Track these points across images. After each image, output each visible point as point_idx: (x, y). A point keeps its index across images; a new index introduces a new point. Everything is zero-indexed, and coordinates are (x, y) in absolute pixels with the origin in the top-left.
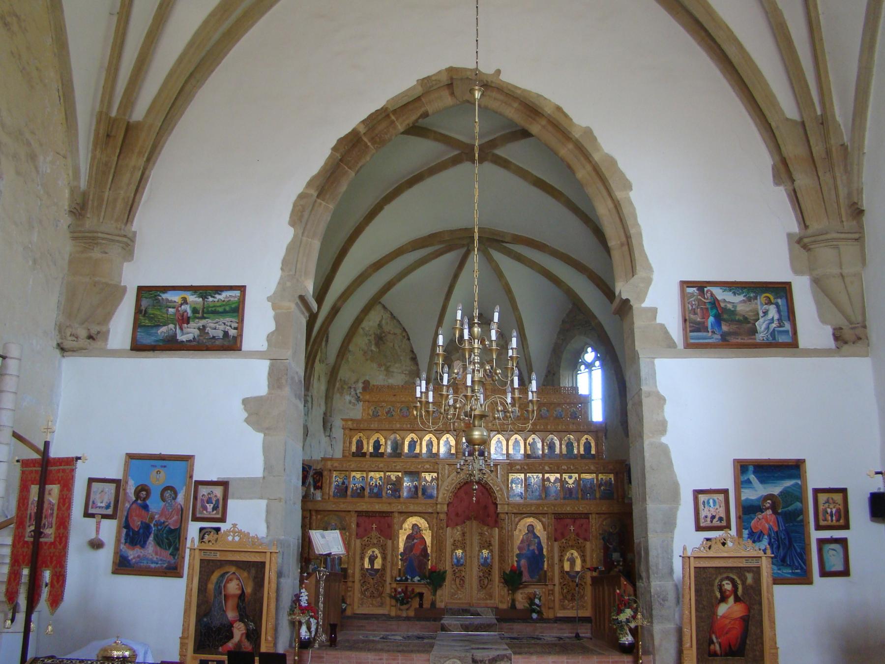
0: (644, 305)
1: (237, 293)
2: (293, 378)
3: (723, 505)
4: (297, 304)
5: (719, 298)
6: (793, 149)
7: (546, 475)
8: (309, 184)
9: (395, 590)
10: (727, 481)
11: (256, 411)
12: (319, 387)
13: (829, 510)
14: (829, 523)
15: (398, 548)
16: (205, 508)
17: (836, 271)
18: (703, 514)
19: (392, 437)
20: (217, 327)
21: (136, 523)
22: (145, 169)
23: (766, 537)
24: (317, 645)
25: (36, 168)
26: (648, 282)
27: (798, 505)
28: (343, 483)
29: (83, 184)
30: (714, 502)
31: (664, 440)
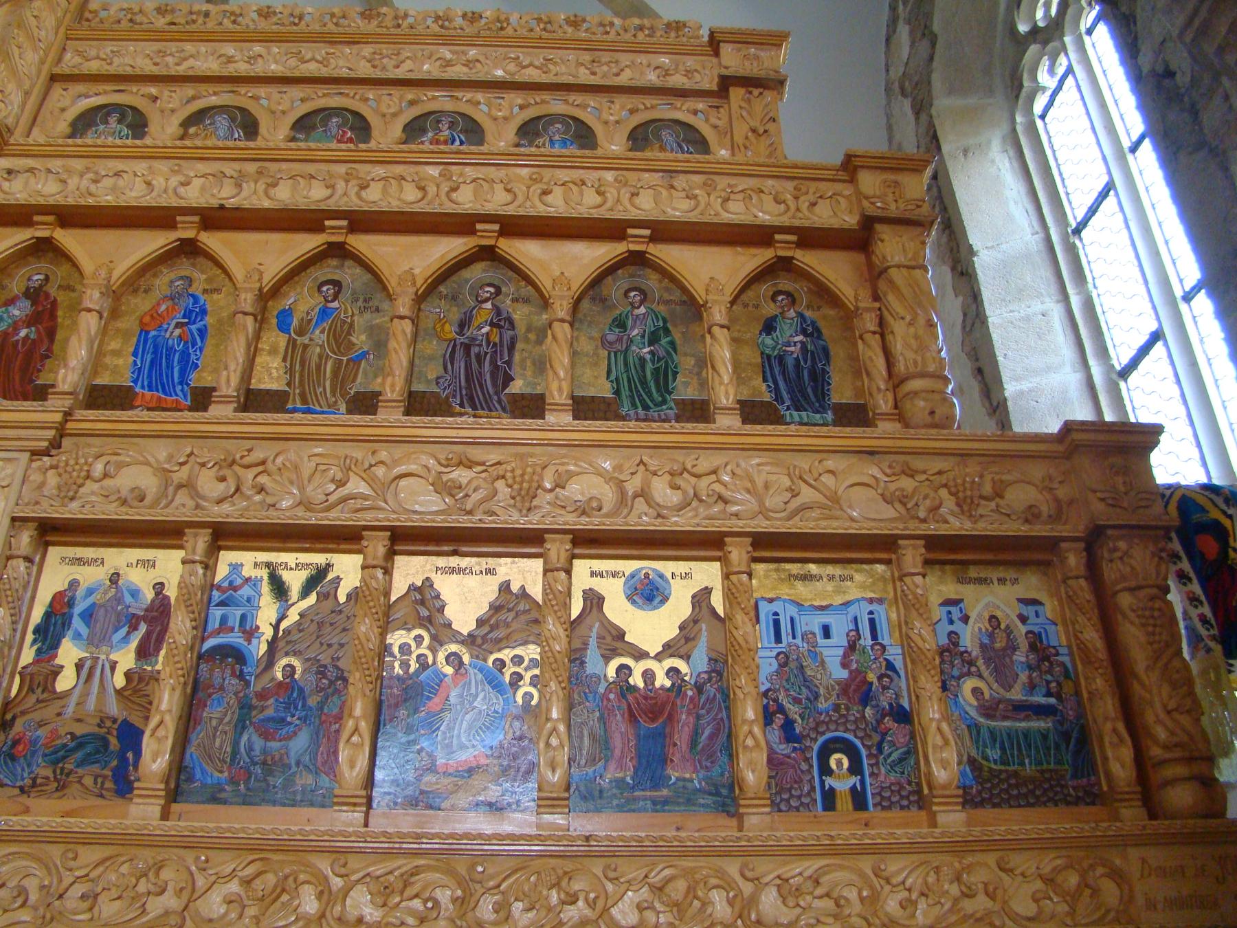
7: (409, 570)
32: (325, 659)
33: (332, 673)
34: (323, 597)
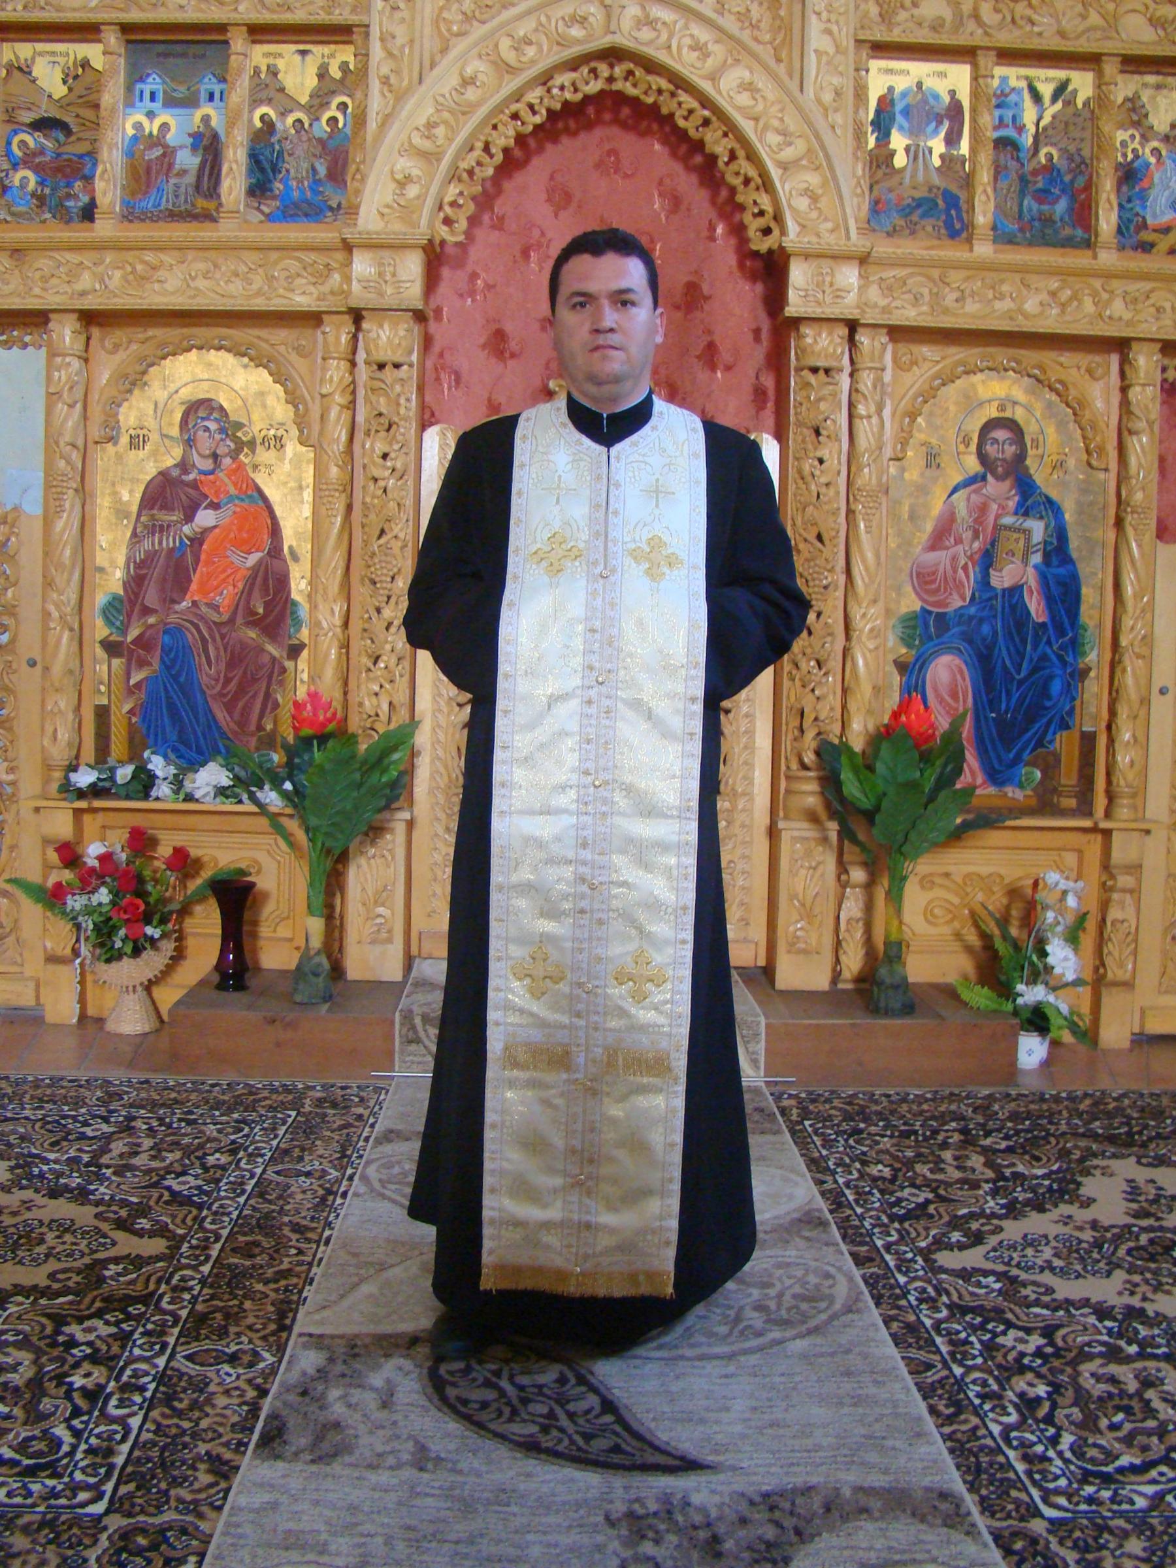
9: (69, 855)
32: (1072, 148)
33: (1078, 159)
34: (1067, 103)
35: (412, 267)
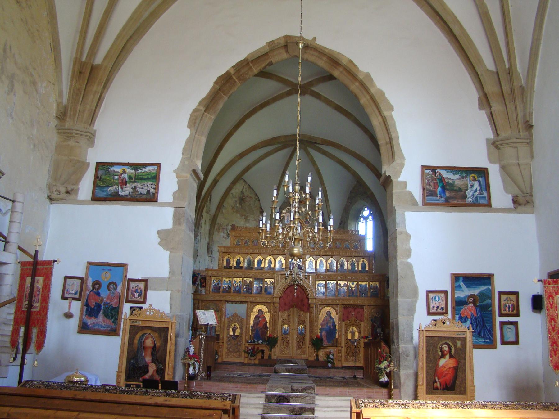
0: (399, 180)
1: (156, 168)
2: (188, 219)
3: (444, 300)
4: (191, 175)
5: (445, 176)
6: (491, 88)
8: (200, 104)
10: (447, 286)
11: (165, 238)
12: (205, 227)
13: (507, 305)
14: (507, 312)
15: (250, 323)
16: (134, 295)
17: (514, 161)
18: (431, 305)
19: (248, 257)
20: (143, 188)
21: (93, 303)
22: (102, 93)
23: (469, 320)
24: (199, 378)
25: (36, 90)
26: (402, 165)
27: (489, 301)
28: (218, 284)
29: (65, 101)
30: (439, 298)
31: (409, 260)
35: (278, 299)
